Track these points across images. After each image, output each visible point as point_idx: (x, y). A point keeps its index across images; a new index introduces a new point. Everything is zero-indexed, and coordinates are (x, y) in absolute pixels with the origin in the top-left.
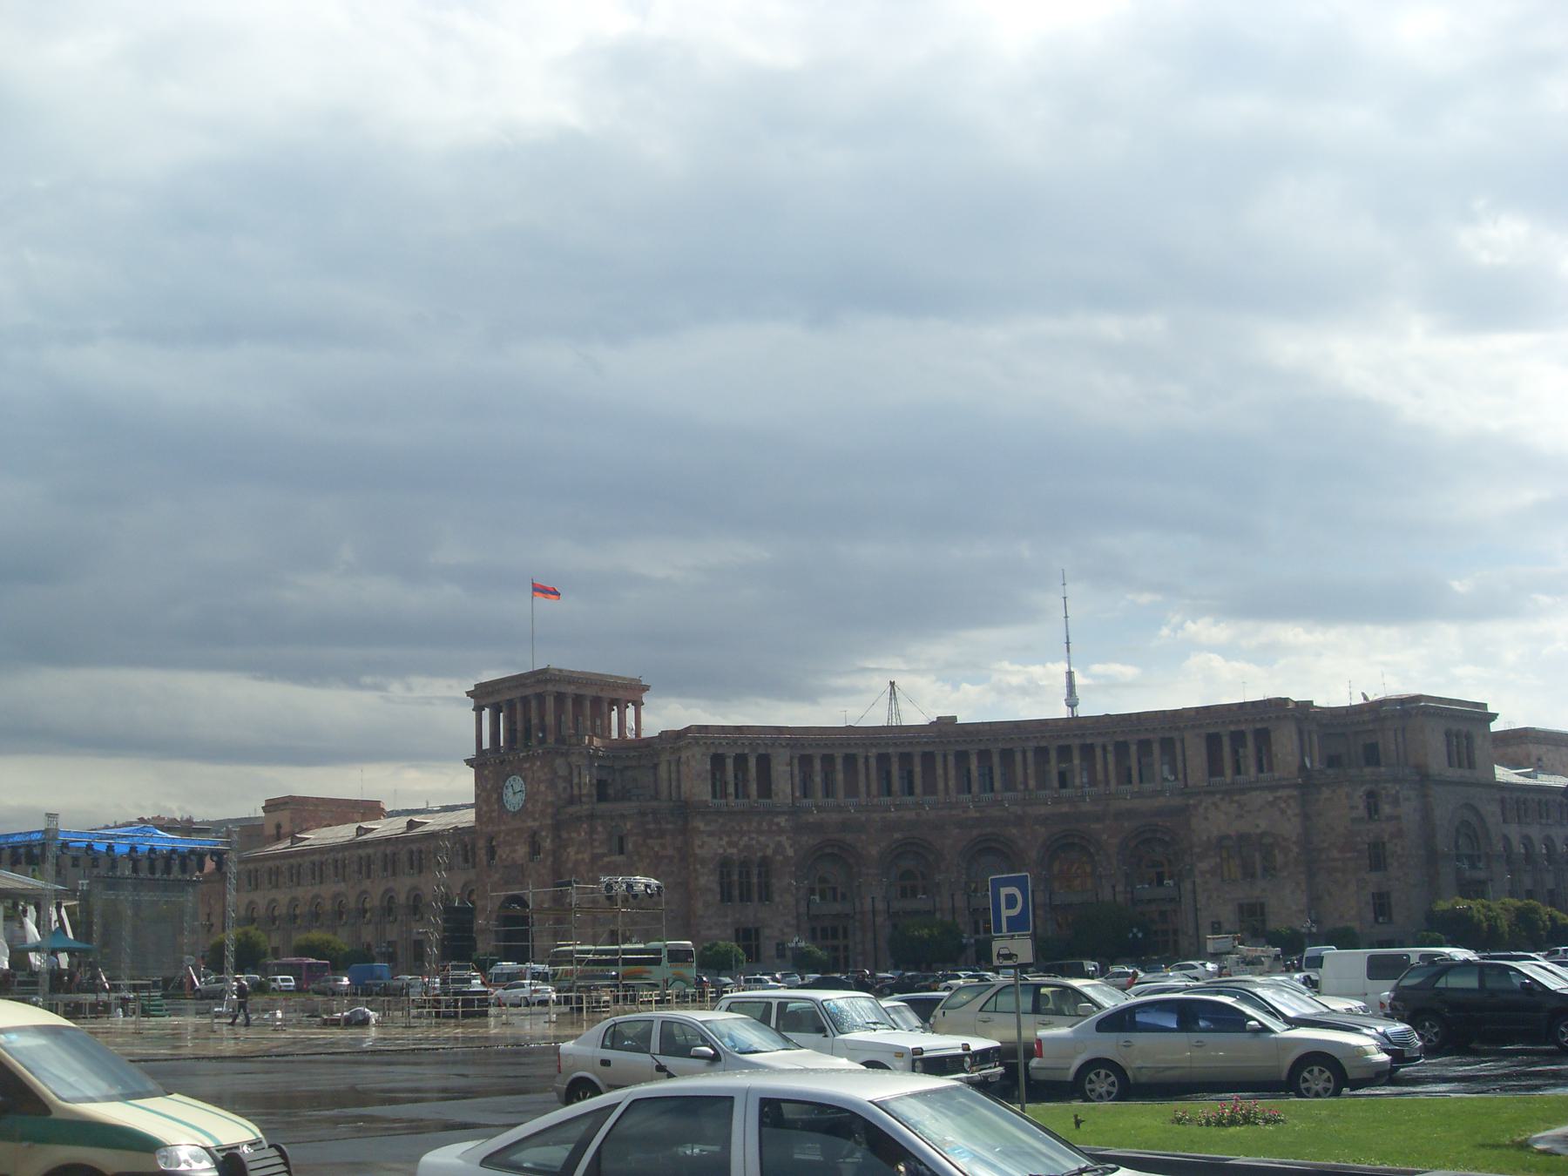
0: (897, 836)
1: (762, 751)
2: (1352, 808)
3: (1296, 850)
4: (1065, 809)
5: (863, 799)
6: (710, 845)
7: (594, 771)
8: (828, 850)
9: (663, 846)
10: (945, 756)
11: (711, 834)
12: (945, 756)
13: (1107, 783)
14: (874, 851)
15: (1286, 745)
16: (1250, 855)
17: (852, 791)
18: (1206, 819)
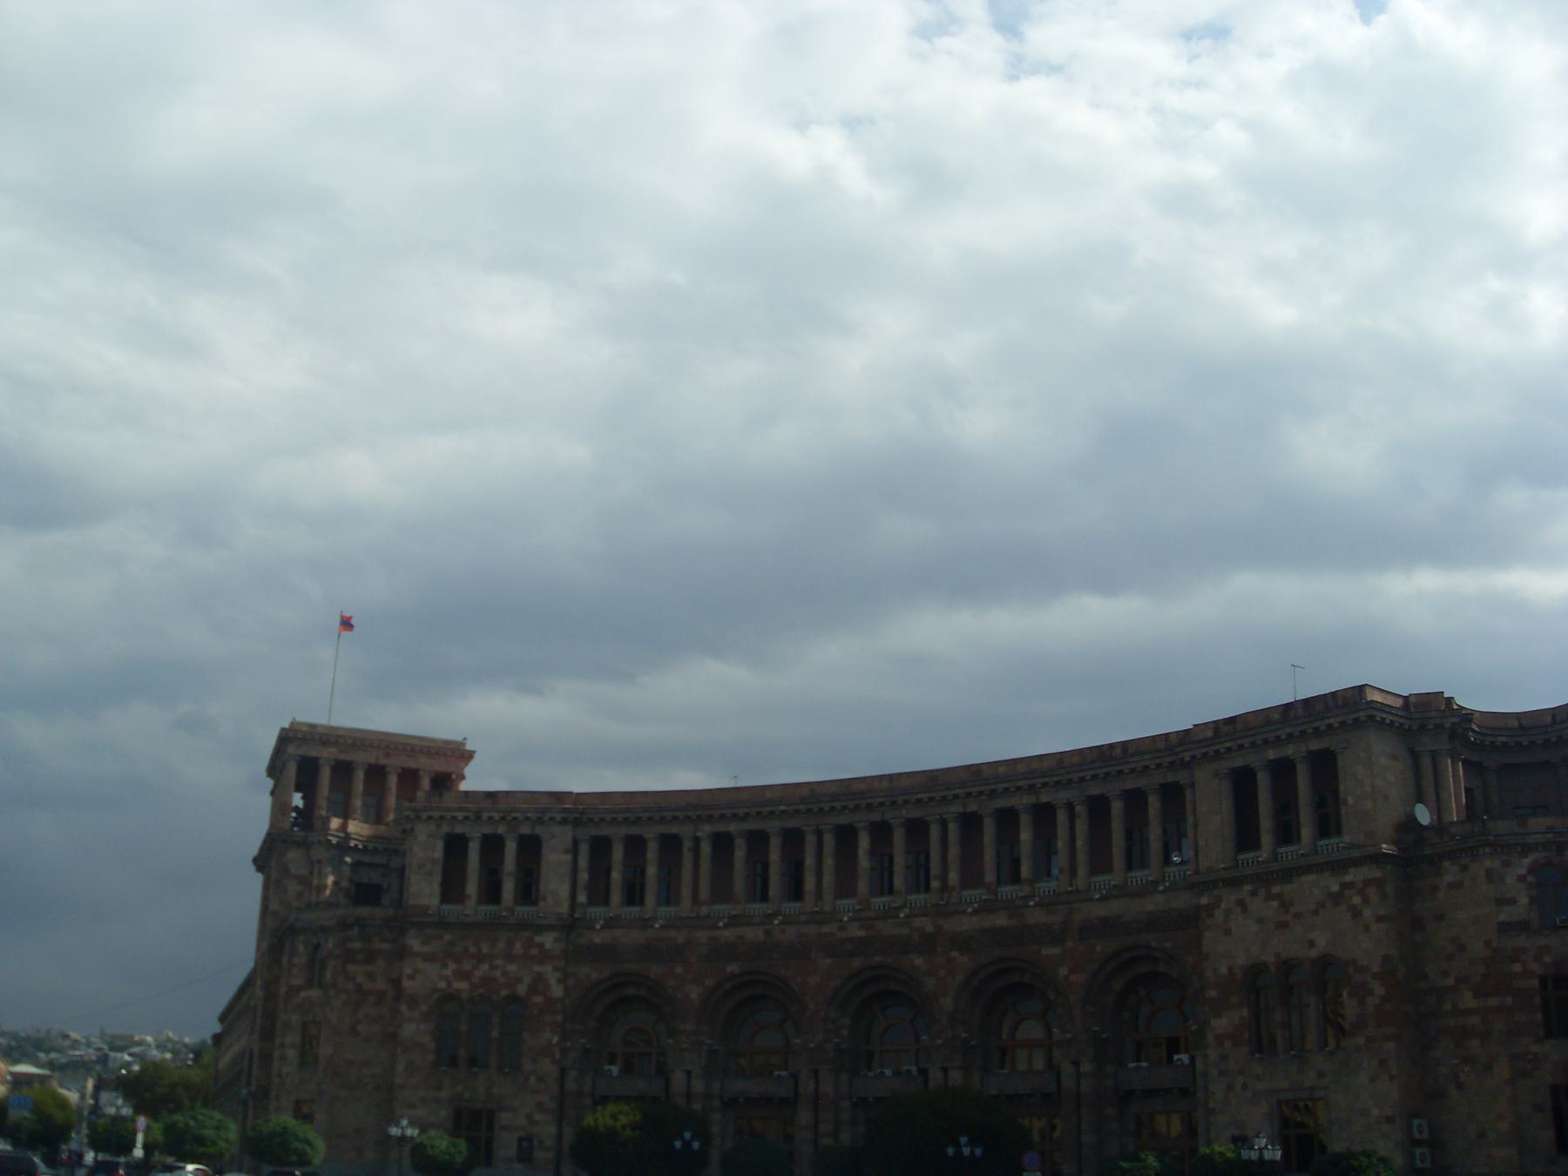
0: (732, 968)
1: (525, 830)
2: (1502, 902)
3: (1379, 990)
4: (1001, 920)
5: (685, 906)
6: (427, 975)
7: (346, 871)
8: (631, 991)
9: (371, 977)
10: (819, 835)
11: (429, 958)
12: (819, 835)
13: (1073, 873)
14: (694, 992)
15: (1376, 782)
16: (1287, 998)
17: (669, 895)
18: (1227, 932)
